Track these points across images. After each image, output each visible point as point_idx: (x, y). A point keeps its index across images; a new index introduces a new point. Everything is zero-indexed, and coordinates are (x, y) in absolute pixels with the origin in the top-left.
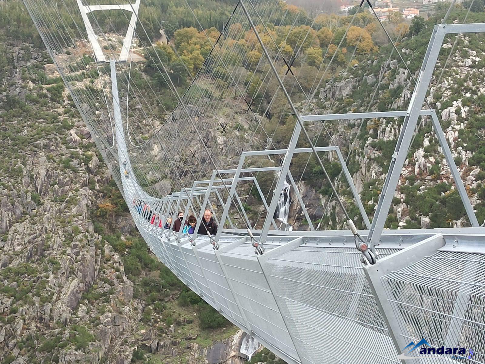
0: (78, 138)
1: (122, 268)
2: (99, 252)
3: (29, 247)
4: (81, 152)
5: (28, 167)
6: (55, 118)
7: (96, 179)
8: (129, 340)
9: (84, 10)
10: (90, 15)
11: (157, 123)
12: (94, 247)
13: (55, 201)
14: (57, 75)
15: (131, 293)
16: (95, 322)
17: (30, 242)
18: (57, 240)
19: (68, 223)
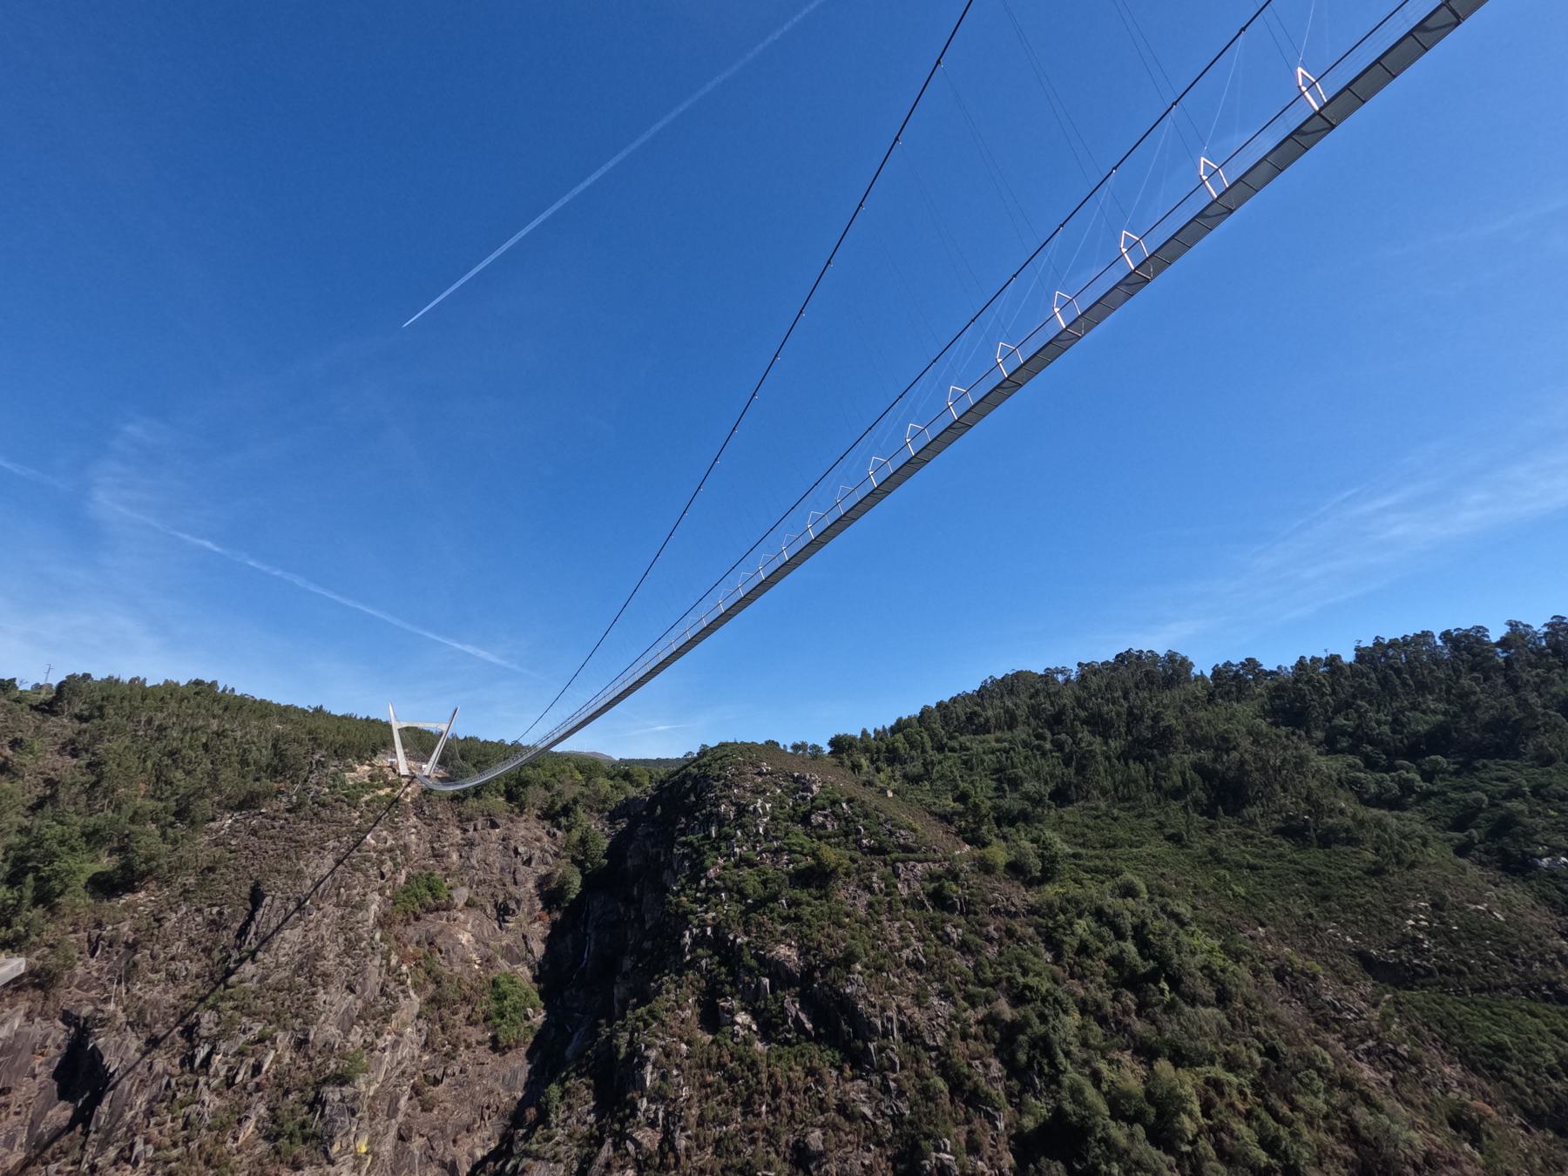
0: (373, 842)
1: (409, 982)
2: (384, 962)
3: (298, 957)
4: (375, 855)
5: (310, 870)
6: (349, 821)
7: (387, 885)
8: (409, 1070)
11: (458, 832)
12: (379, 957)
13: (337, 905)
15: (416, 1011)
16: (370, 1047)
17: (299, 952)
18: (331, 952)
19: (350, 929)
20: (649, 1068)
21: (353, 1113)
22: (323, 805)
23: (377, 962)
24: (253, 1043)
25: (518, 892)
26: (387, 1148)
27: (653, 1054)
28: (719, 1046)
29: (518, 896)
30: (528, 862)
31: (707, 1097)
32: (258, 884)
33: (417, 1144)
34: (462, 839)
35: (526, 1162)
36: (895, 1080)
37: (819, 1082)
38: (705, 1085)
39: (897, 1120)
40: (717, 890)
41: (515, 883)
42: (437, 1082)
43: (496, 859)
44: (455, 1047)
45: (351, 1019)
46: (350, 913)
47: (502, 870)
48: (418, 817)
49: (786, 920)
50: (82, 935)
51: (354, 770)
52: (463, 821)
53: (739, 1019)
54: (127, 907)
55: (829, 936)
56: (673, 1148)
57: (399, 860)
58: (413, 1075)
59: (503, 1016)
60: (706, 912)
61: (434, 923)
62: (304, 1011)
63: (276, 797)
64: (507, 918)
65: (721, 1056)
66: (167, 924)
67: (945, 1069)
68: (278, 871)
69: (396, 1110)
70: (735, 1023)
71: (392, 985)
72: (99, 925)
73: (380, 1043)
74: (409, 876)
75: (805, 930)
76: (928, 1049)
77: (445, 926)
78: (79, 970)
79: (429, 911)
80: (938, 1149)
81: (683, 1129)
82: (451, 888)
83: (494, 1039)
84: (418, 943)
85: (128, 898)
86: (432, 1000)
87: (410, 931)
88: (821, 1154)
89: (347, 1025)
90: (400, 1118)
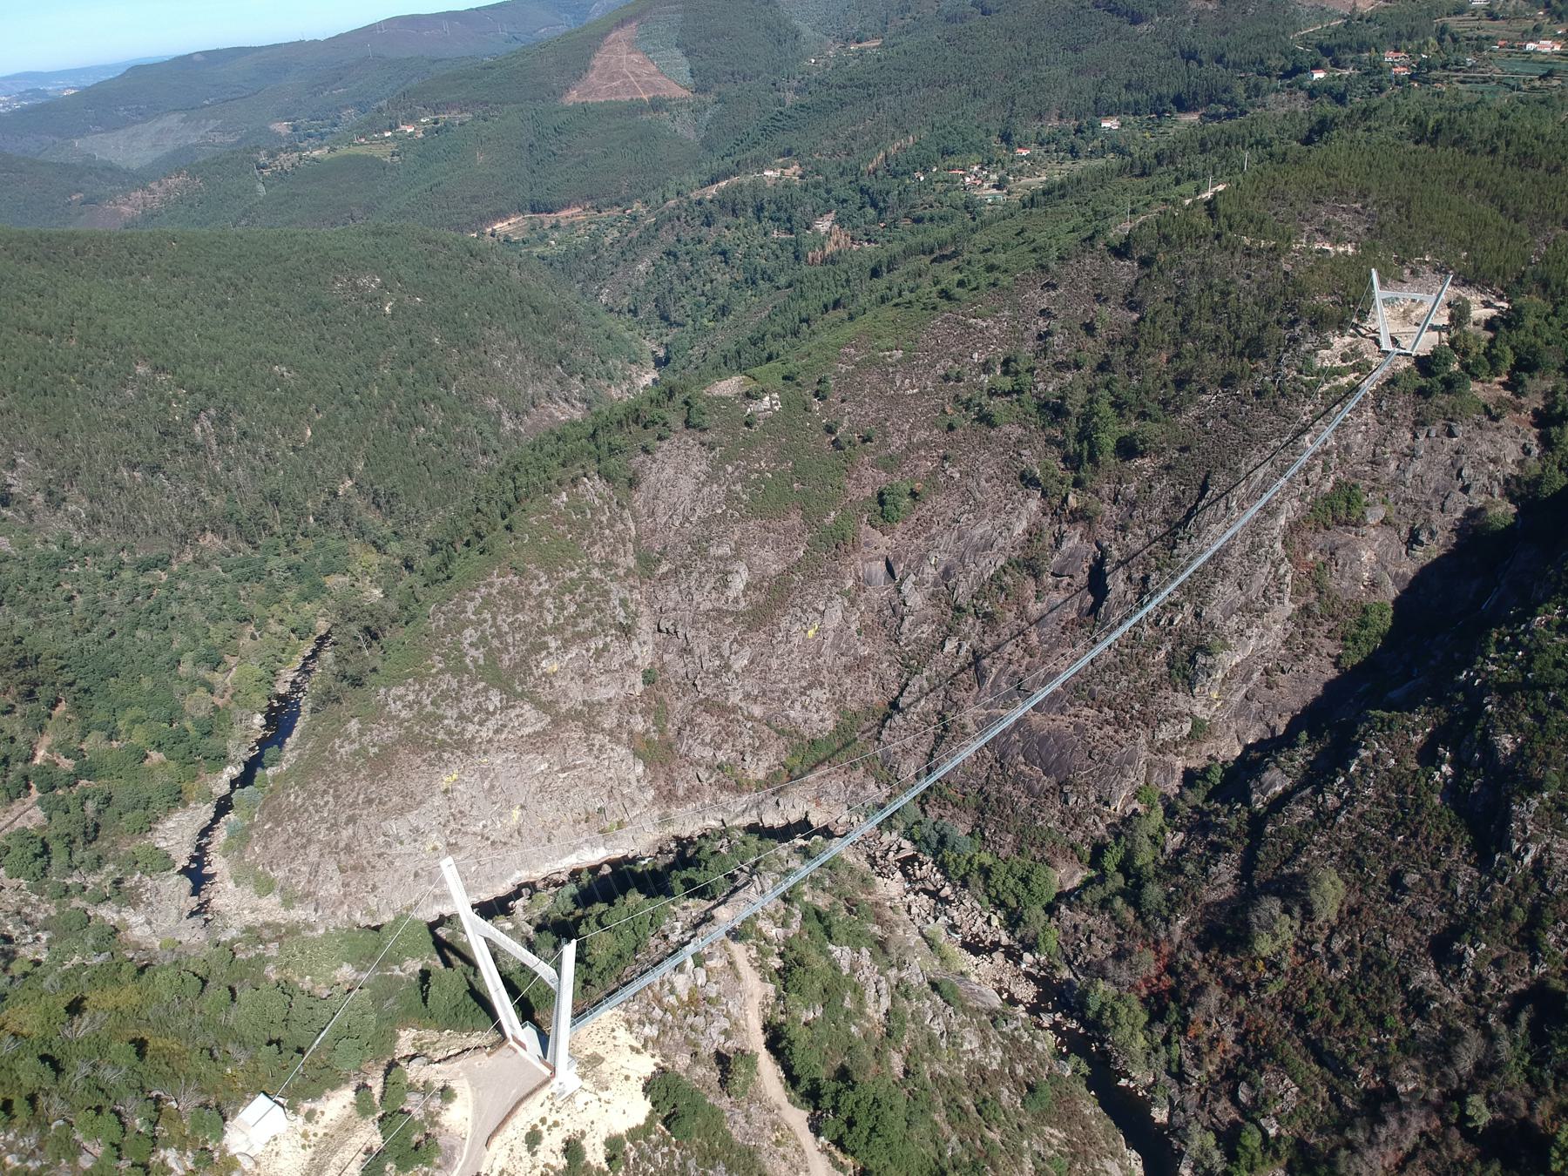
9: (1379, 293)
10: (1384, 301)
11: (1409, 436)
12: (1269, 565)
14: (1327, 364)
16: (1241, 633)
20: (1356, 762)
21: (1209, 676)
22: (1283, 395)
23: (1265, 570)
24: (1170, 604)
25: (1438, 520)
26: (1238, 698)
27: (1364, 753)
28: (1414, 778)
29: (1434, 527)
30: (1465, 489)
31: (1379, 804)
32: (1207, 477)
33: (1255, 706)
34: (1408, 447)
35: (1272, 765)
36: (1493, 888)
37: (1447, 849)
38: (1383, 795)
39: (1472, 910)
40: (1517, 645)
41: (1442, 510)
42: (1283, 672)
43: (1436, 477)
44: (1306, 651)
45: (1232, 609)
46: (1265, 518)
47: (1436, 491)
48: (1375, 412)
49: (1537, 715)
50: (1112, 486)
51: (1328, 346)
52: (1420, 423)
53: (1444, 768)
54: (1139, 469)
55: (1548, 755)
56: (1335, 819)
57: (1332, 465)
58: (1269, 660)
59: (1356, 643)
60: (1494, 661)
61: (1339, 536)
62: (1204, 594)
63: (1251, 376)
64: (1415, 546)
65: (1407, 785)
66: (1155, 492)
67: (1535, 912)
68: (1222, 465)
69: (1250, 679)
70: (1438, 769)
71: (1273, 590)
72: (1120, 483)
73: (1248, 633)
74: (1337, 483)
75: (1537, 737)
76: (1543, 888)
77: (1352, 540)
78: (1107, 513)
79: (1339, 524)
80: (1472, 945)
81: (1349, 812)
82: (1367, 505)
83: (1339, 656)
84: (1321, 550)
85: (1139, 461)
86: (1306, 610)
87: (1318, 538)
88: (1408, 889)
89: (1228, 614)
90: (1251, 685)
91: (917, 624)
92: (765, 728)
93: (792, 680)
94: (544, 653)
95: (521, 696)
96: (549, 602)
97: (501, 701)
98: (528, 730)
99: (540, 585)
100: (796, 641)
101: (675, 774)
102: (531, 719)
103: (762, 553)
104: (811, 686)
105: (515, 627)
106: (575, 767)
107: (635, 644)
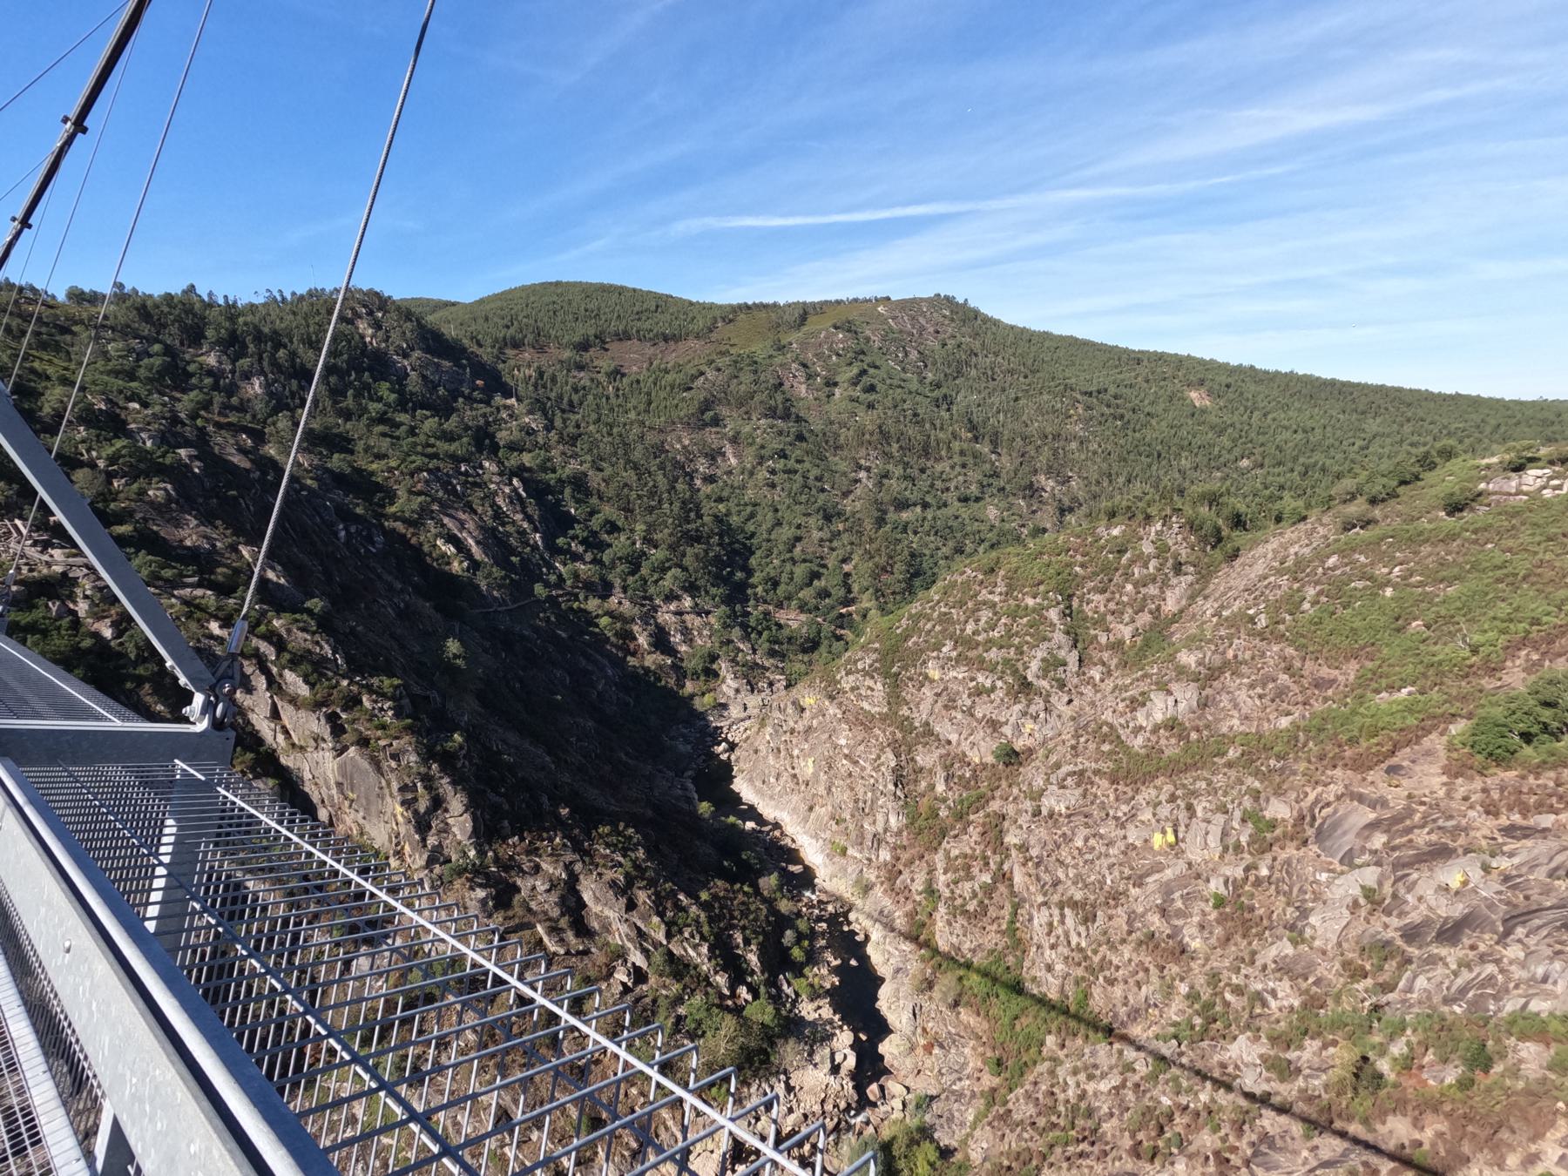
91: (1284, 968)
92: (1008, 908)
93: (1078, 879)
94: (935, 654)
95: (886, 675)
96: (985, 615)
97: (871, 666)
98: (866, 706)
99: (991, 593)
100: (1133, 836)
101: (917, 862)
102: (874, 698)
103: (1242, 695)
104: (1074, 905)
105: (945, 619)
106: (856, 763)
107: (1018, 707)
